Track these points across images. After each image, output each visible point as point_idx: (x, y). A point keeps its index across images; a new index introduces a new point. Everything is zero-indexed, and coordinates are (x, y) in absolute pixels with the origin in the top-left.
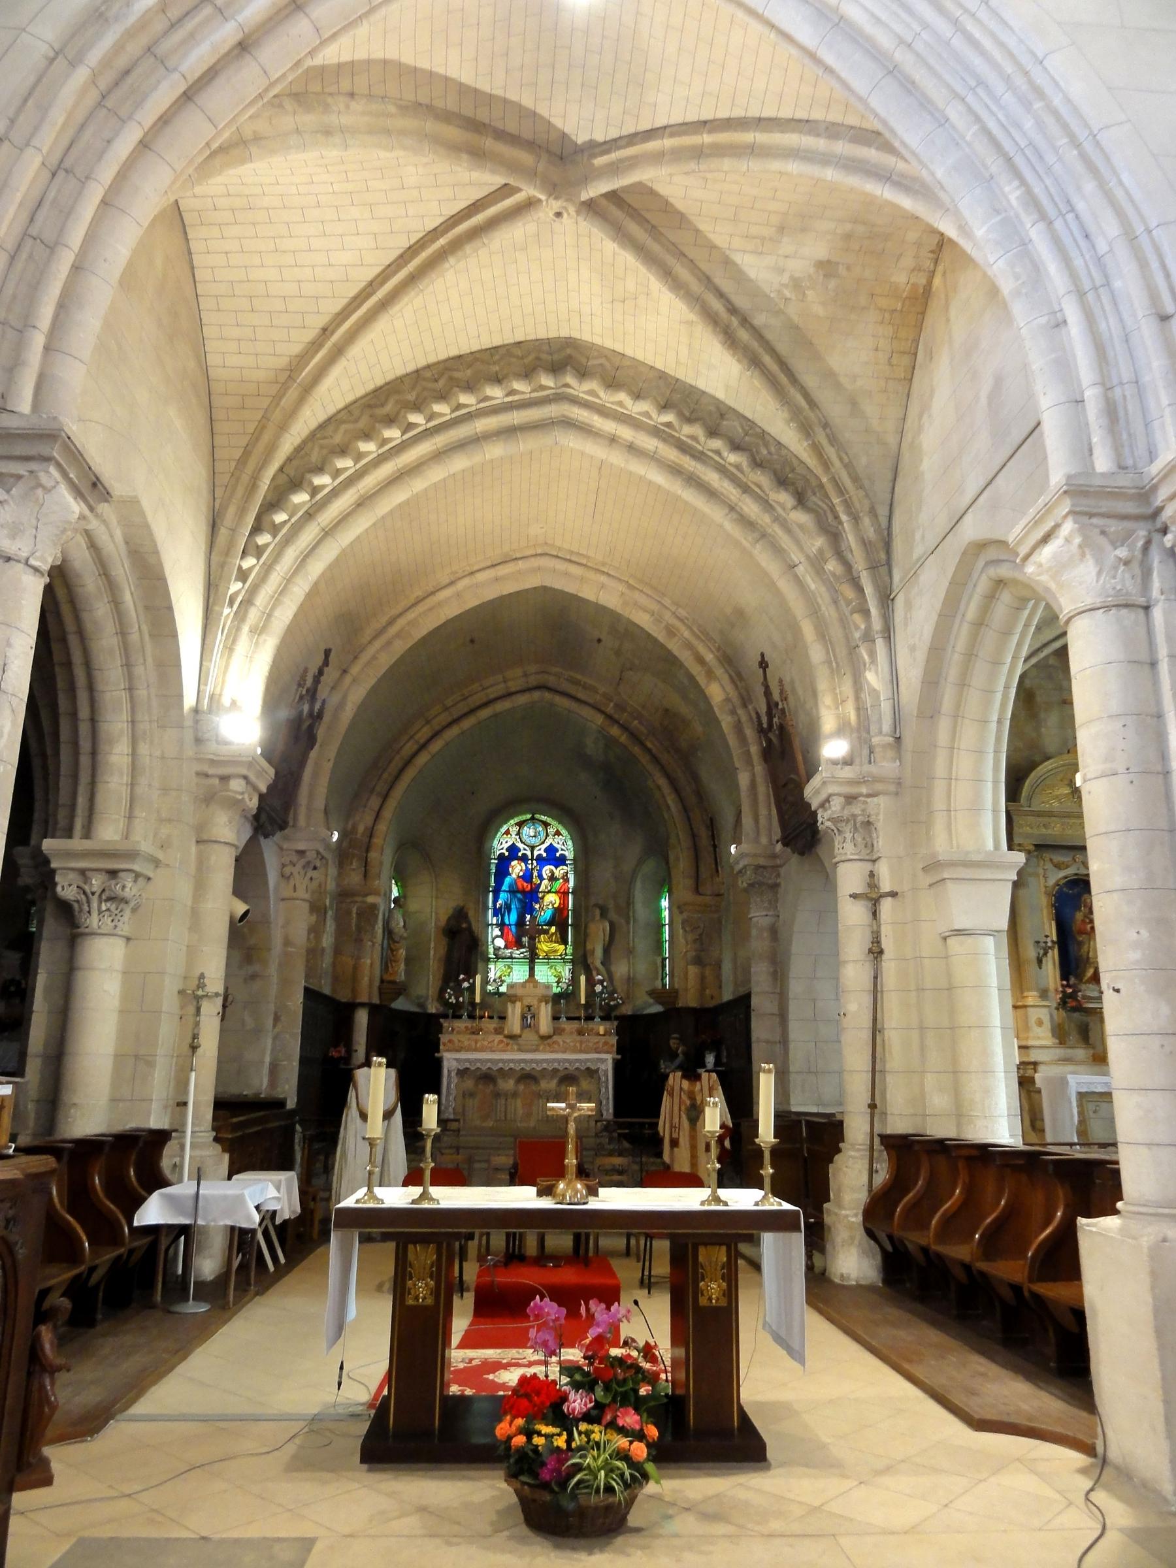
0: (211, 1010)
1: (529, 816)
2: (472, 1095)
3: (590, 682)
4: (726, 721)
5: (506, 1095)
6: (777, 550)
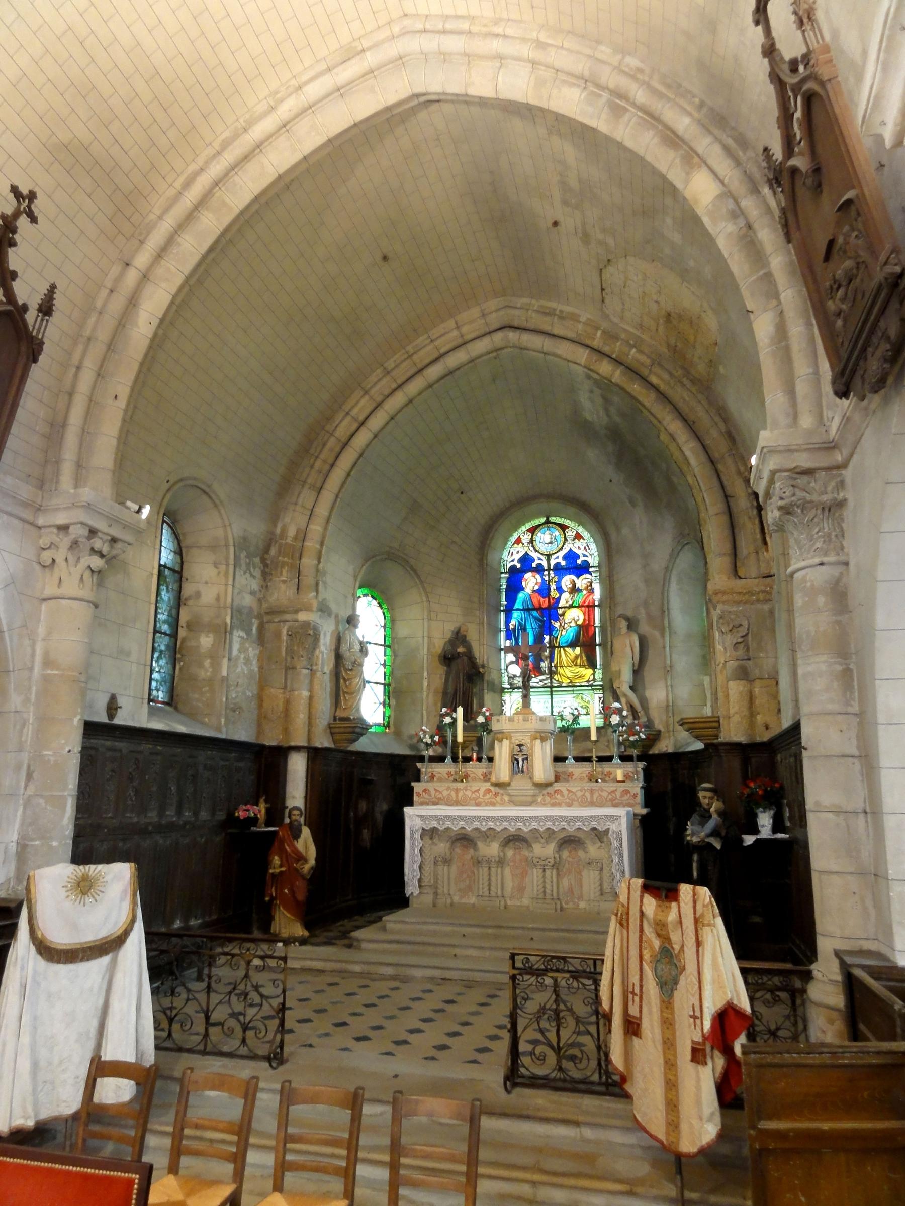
1: (543, 520)
2: (447, 861)
3: (568, 309)
4: (724, 234)
5: (489, 862)
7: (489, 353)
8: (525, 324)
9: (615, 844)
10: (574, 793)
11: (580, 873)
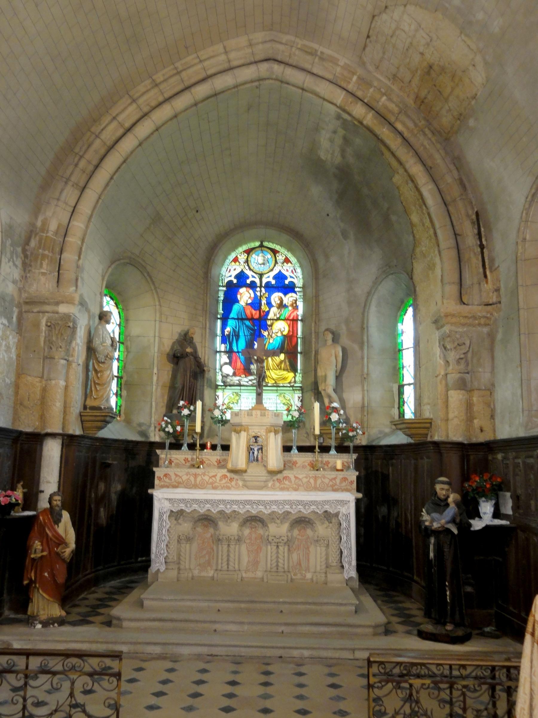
1: (257, 244)
2: (189, 539)
3: (328, 52)
5: (229, 540)
7: (252, 81)
8: (286, 60)
9: (344, 525)
10: (300, 479)
11: (308, 548)
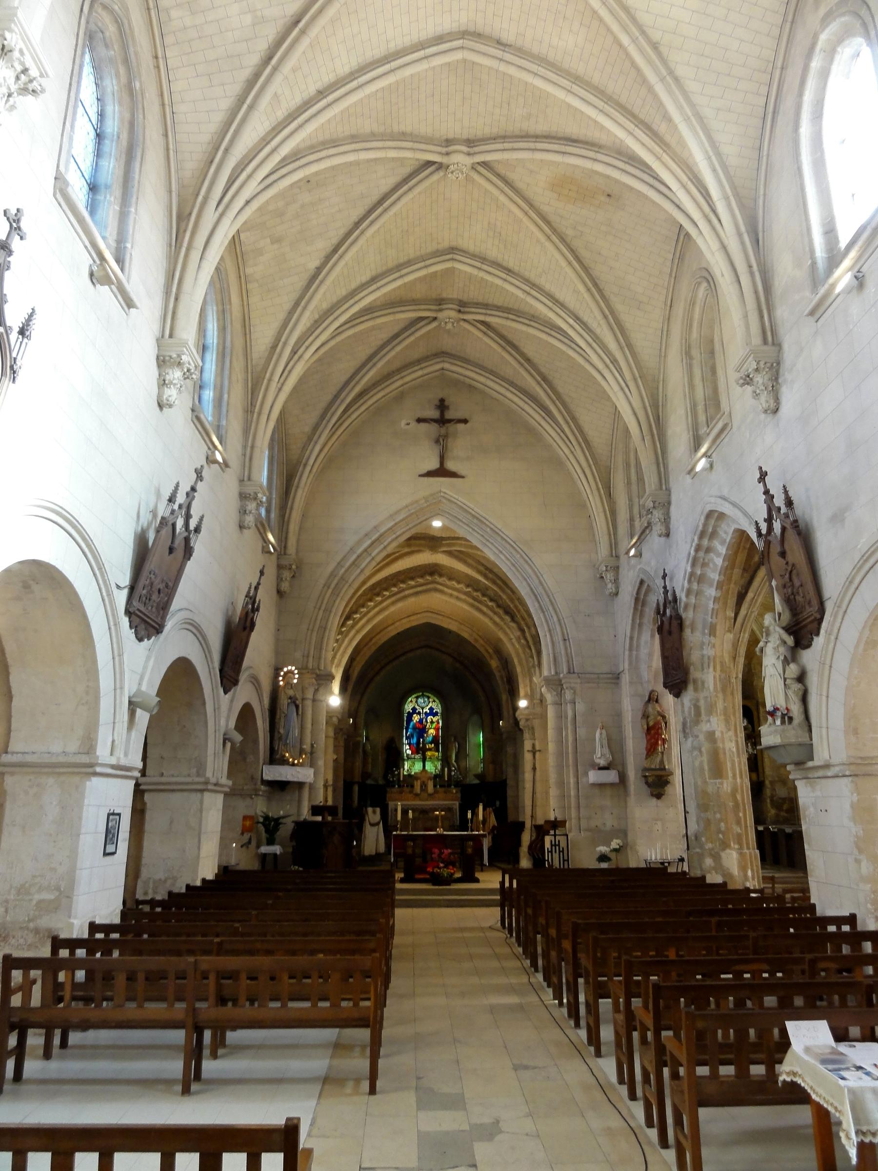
0: (330, 790)
4: (497, 674)
6: (506, 634)
